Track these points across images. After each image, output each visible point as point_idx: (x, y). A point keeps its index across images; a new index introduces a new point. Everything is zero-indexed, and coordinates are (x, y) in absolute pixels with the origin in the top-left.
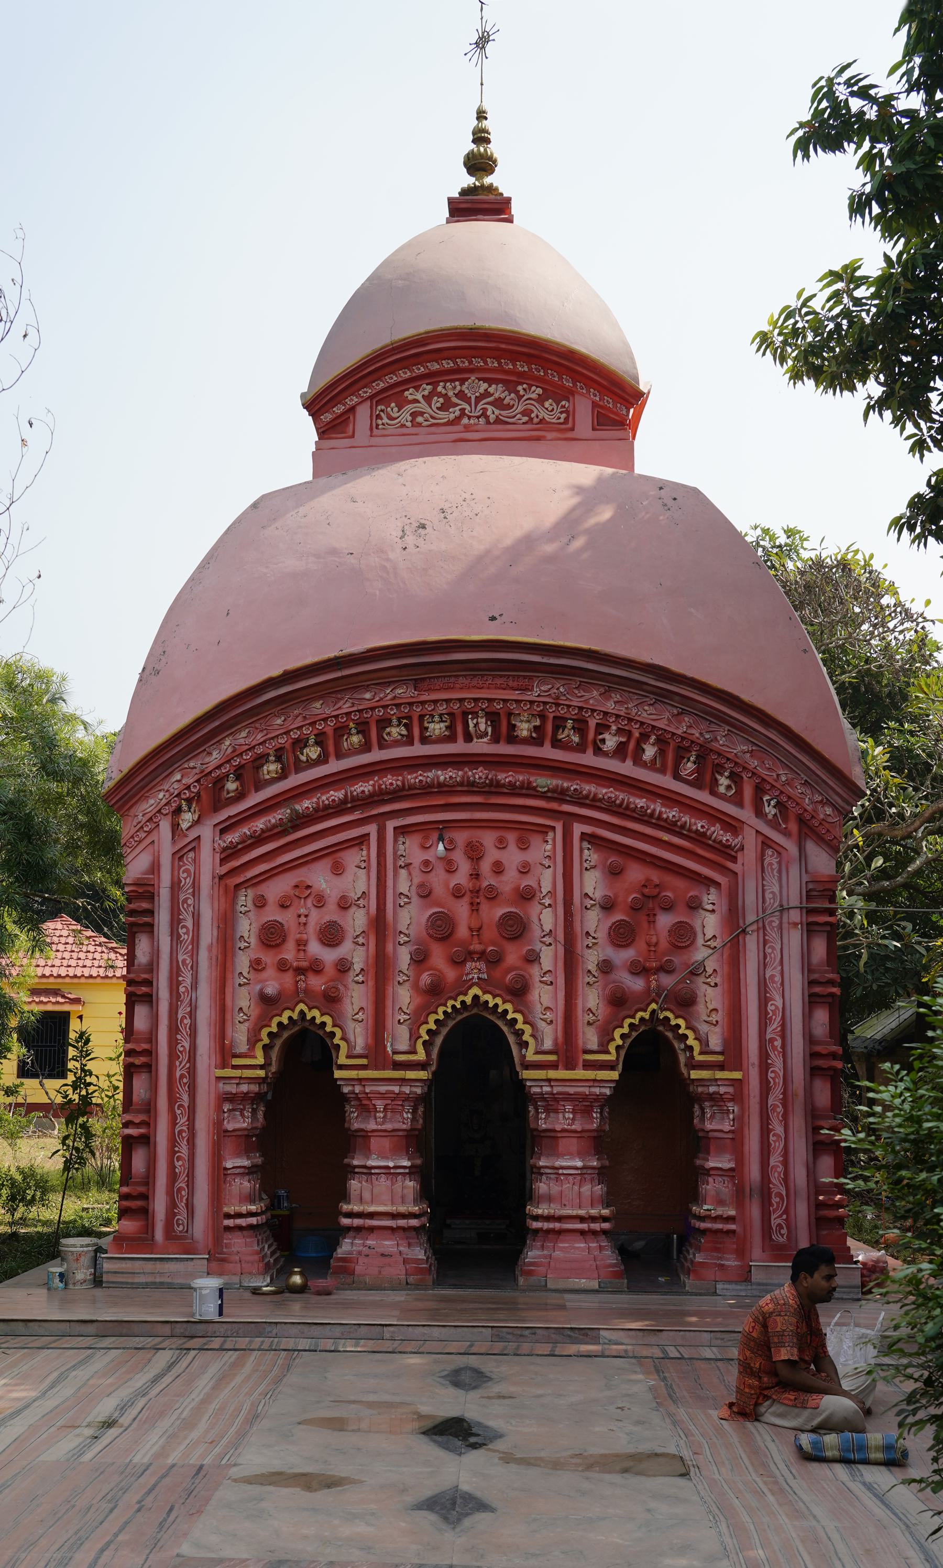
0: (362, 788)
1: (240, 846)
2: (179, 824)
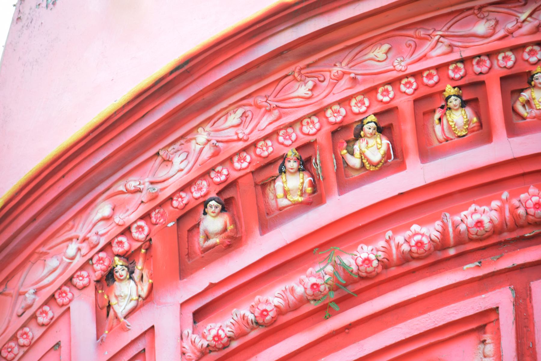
0: (476, 217)
1: (235, 345)
2: (109, 306)
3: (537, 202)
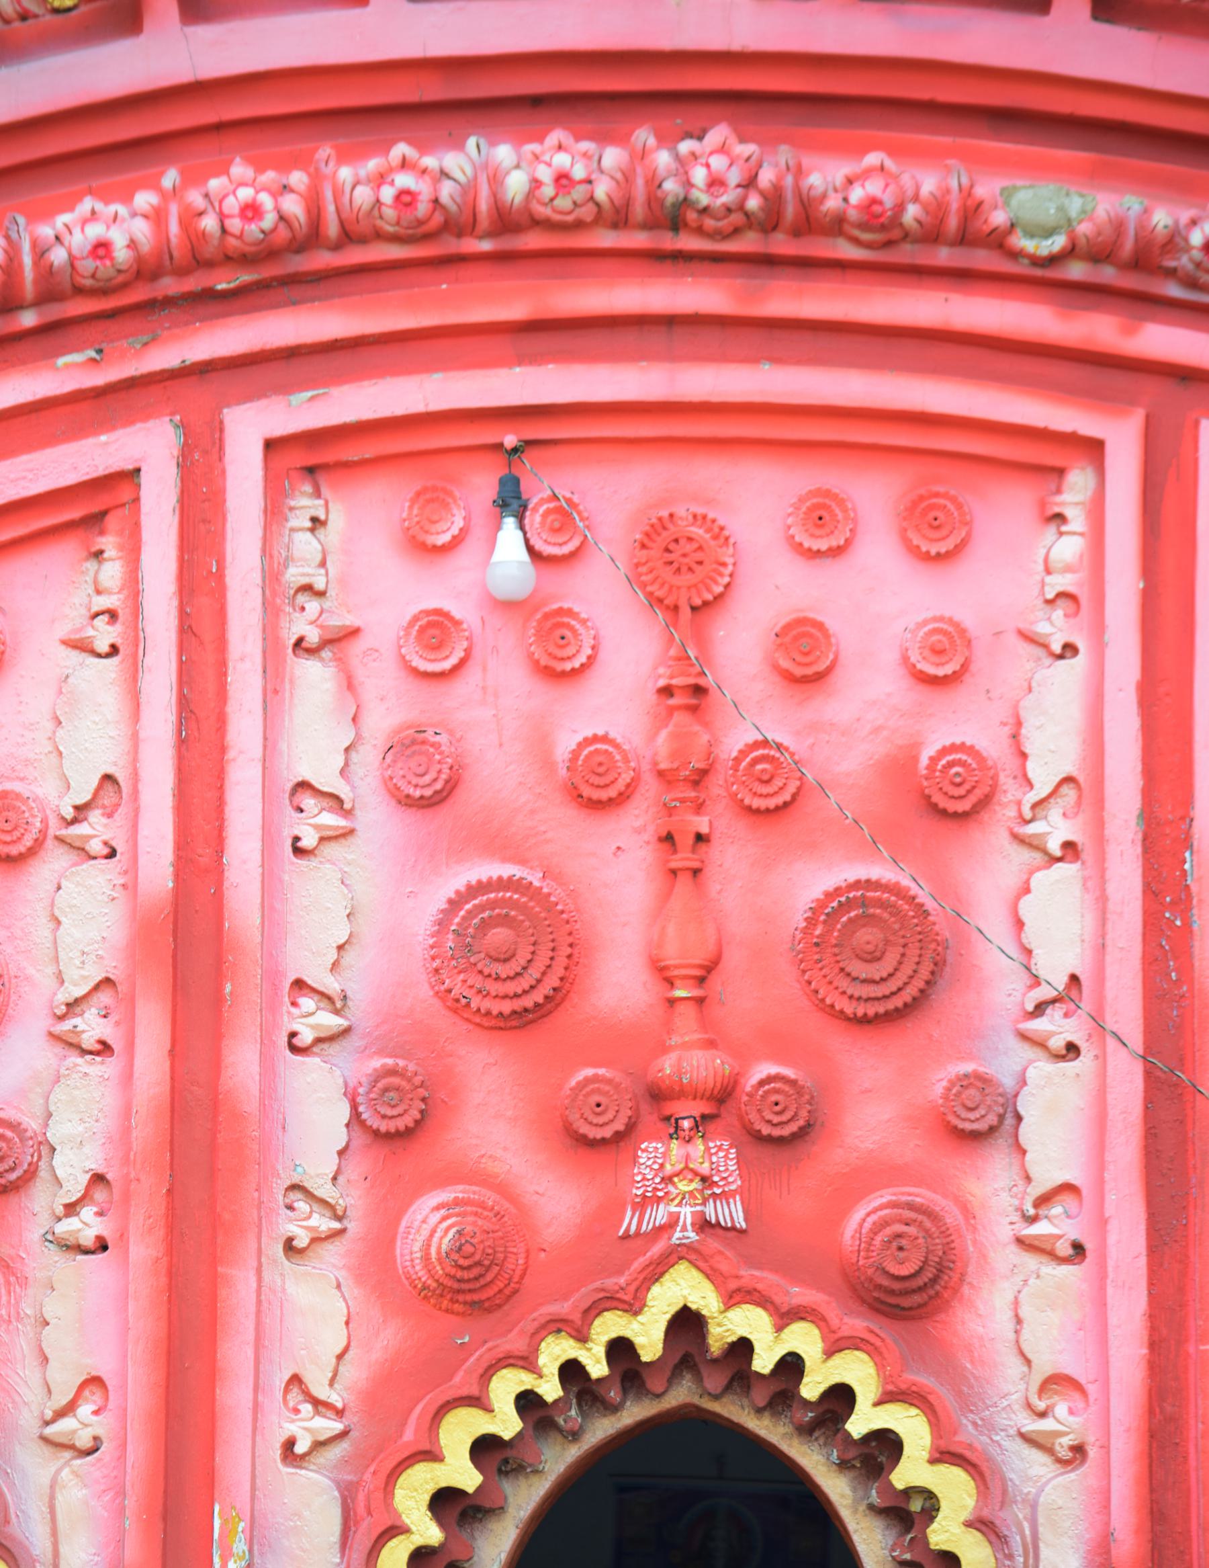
0: (95, 231)
3: (250, 201)
